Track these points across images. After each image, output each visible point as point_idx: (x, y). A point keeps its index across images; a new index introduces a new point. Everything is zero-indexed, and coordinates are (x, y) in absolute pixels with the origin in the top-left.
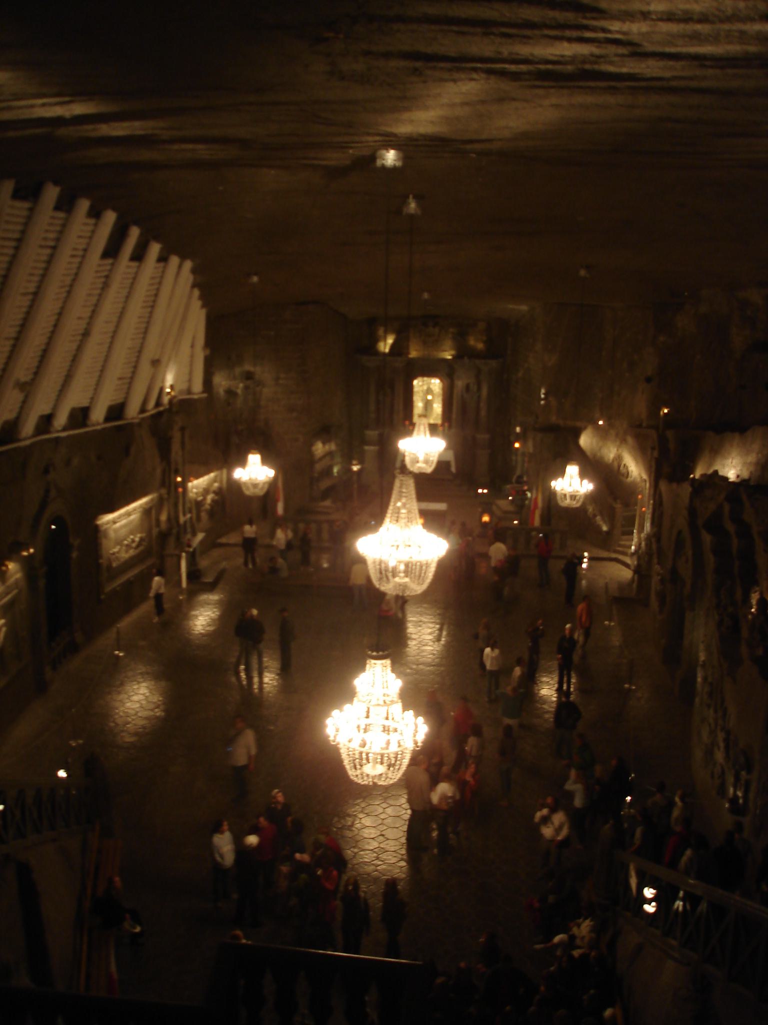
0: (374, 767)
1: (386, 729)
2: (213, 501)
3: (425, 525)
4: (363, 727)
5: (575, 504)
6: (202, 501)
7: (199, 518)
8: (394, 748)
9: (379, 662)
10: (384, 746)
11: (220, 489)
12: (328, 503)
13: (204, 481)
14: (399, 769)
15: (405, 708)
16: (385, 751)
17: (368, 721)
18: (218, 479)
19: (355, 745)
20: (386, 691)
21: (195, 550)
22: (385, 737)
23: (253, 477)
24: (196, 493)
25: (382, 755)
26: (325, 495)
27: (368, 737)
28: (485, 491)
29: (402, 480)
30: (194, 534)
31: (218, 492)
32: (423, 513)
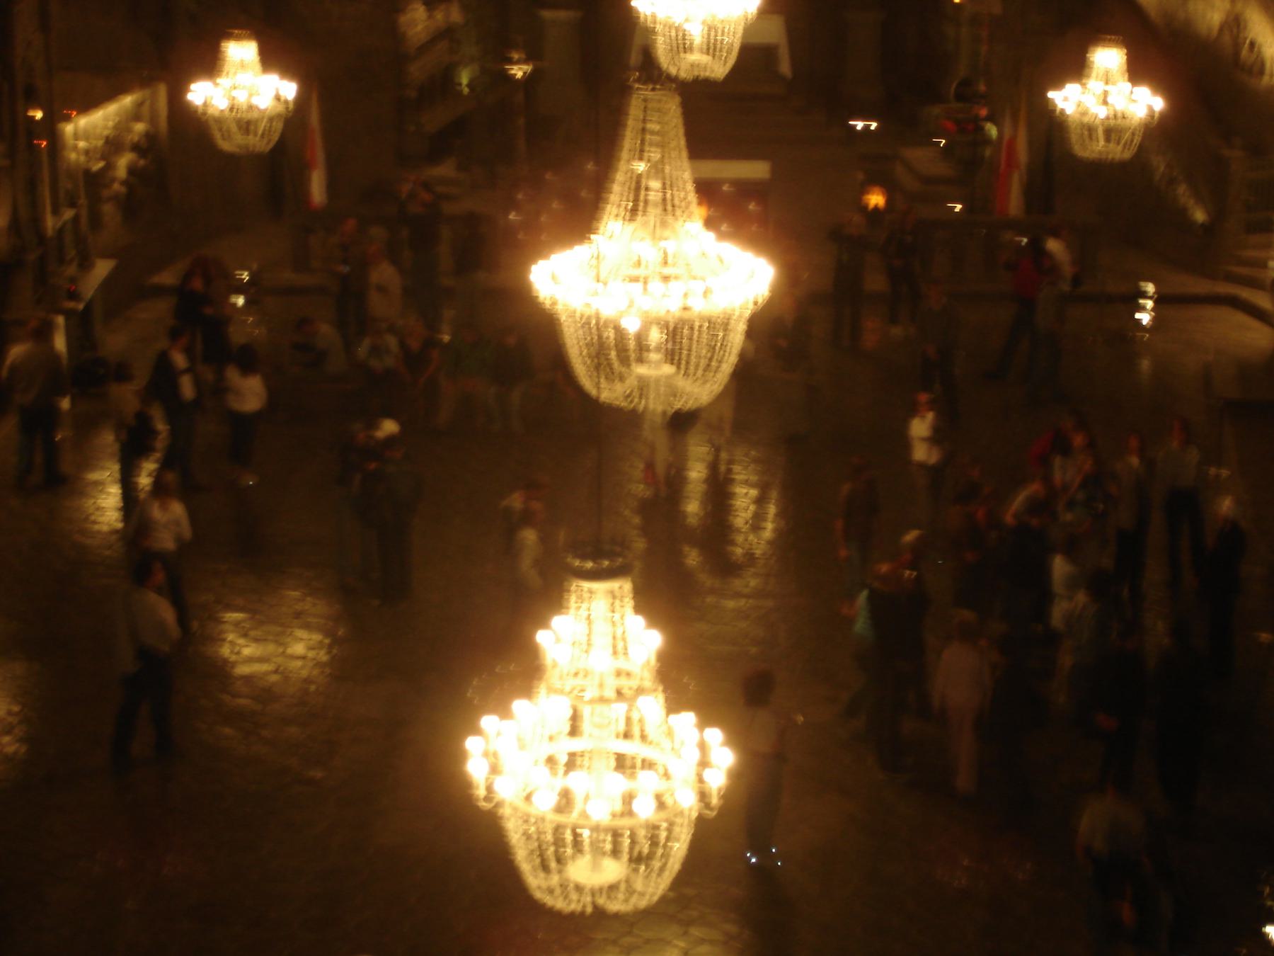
0: (595, 866)
1: (622, 763)
2: (132, 170)
3: (709, 223)
4: (563, 759)
5: (1118, 152)
6: (103, 170)
7: (96, 221)
8: (645, 810)
9: (600, 587)
10: (618, 807)
11: (150, 137)
12: (445, 170)
13: (106, 119)
14: (662, 869)
15: (674, 705)
16: (626, 822)
17: (576, 745)
18: (146, 109)
19: (544, 804)
20: (622, 664)
21: (88, 307)
22: (620, 783)
23: (242, 98)
24: (87, 152)
25: (616, 835)
26: (439, 147)
27: (577, 782)
28: (874, 125)
29: (645, 100)
30: (85, 264)
31: (146, 147)
32: (706, 191)
